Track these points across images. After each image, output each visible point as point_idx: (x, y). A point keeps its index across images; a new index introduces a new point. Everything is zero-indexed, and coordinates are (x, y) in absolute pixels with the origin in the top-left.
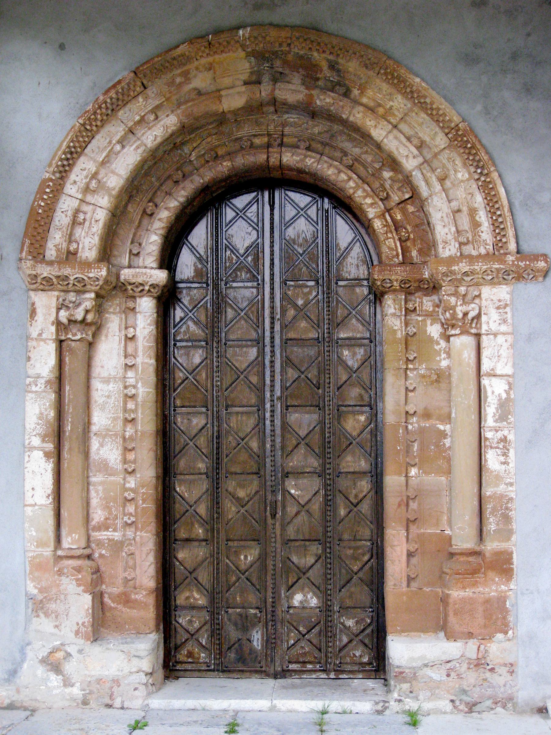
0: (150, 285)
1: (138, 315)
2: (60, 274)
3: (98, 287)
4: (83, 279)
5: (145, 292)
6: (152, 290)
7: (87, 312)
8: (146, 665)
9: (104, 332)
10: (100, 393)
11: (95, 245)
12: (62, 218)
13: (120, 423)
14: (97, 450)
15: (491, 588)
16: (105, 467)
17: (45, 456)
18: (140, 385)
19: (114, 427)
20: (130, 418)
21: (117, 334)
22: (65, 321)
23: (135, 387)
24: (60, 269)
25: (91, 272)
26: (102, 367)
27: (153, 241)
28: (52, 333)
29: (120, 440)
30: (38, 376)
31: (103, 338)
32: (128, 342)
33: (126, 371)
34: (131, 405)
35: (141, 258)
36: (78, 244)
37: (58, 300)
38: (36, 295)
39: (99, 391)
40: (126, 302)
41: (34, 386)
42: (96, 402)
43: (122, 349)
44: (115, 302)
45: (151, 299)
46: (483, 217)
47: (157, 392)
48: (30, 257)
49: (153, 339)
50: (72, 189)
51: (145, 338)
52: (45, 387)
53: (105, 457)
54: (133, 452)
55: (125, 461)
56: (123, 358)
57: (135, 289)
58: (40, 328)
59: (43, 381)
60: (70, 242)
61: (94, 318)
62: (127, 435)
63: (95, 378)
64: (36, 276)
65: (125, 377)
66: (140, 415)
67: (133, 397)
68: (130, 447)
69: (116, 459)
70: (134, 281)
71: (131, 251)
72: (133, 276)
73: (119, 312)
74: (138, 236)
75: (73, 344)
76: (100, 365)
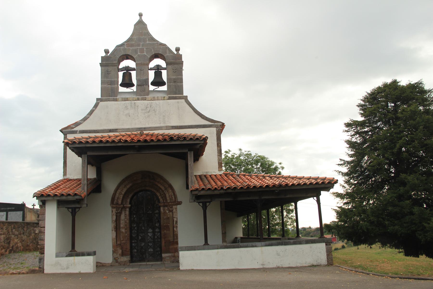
8: (129, 259)
12: (116, 198)
15: (175, 246)
16: (122, 232)
27: (129, 200)
46: (173, 196)
50: (117, 194)
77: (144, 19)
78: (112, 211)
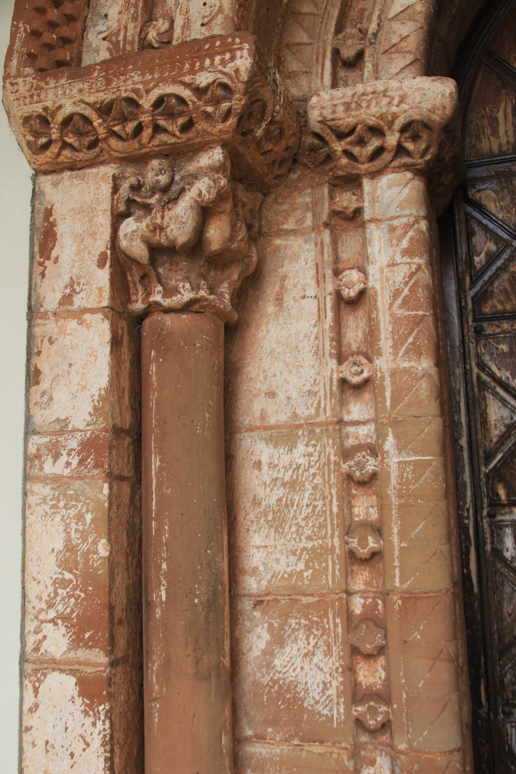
0: (403, 130)
1: (371, 227)
2: (107, 97)
3: (232, 121)
4: (181, 100)
5: (386, 156)
6: (410, 146)
7: (205, 212)
9: (271, 290)
10: (266, 475)
11: (221, 9)
13: (333, 567)
14: (264, 652)
17: (81, 694)
18: (390, 443)
19: (314, 578)
20: (363, 552)
21: (311, 292)
22: (138, 250)
23: (374, 450)
24: (108, 82)
25: (202, 68)
26: (271, 394)
28: (100, 289)
29: (335, 624)
30: (63, 428)
31: (270, 309)
32: (343, 313)
33: (342, 403)
34: (364, 508)
35: (368, 67)
36: (172, 22)
37: (115, 189)
38: (55, 185)
39: (265, 468)
40: (332, 198)
41: (50, 460)
42: (256, 503)
43: (328, 334)
44: (299, 200)
45: (409, 175)
47: (445, 466)
48: (28, 70)
49: (422, 294)
51: (396, 294)
52: (81, 462)
53: (291, 676)
54: (381, 661)
55: (355, 694)
56: (333, 363)
57: (356, 150)
58: (66, 279)
59: (74, 444)
60: (149, 18)
61: (232, 238)
62: (358, 605)
63: (251, 429)
64: (44, 120)
65: (341, 422)
66: (395, 539)
67: (369, 482)
68: (368, 647)
69: (326, 686)
70: (351, 121)
71: (336, 52)
72: (347, 106)
73: (314, 228)
74: (354, 14)
75: (168, 320)
76: (264, 388)
78: (44, 238)
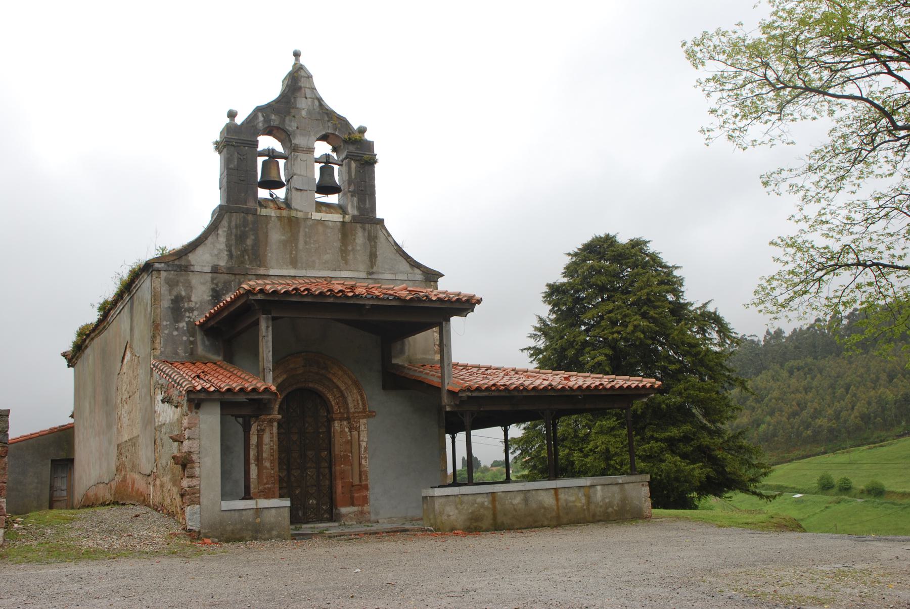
16: (266, 468)
77: (303, 61)
